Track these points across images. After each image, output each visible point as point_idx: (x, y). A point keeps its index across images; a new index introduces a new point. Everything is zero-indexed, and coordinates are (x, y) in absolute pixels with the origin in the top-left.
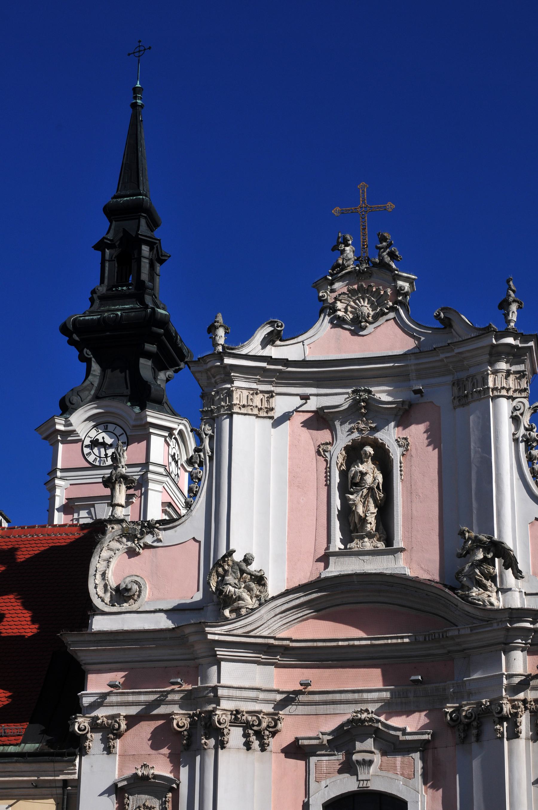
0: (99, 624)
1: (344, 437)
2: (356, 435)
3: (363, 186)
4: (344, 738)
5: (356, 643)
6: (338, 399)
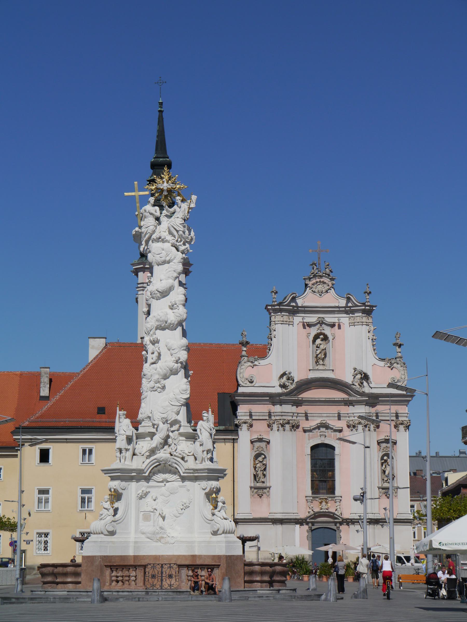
0: (241, 390)
1: (314, 331)
2: (319, 331)
4: (318, 427)
5: (321, 399)
6: (312, 318)
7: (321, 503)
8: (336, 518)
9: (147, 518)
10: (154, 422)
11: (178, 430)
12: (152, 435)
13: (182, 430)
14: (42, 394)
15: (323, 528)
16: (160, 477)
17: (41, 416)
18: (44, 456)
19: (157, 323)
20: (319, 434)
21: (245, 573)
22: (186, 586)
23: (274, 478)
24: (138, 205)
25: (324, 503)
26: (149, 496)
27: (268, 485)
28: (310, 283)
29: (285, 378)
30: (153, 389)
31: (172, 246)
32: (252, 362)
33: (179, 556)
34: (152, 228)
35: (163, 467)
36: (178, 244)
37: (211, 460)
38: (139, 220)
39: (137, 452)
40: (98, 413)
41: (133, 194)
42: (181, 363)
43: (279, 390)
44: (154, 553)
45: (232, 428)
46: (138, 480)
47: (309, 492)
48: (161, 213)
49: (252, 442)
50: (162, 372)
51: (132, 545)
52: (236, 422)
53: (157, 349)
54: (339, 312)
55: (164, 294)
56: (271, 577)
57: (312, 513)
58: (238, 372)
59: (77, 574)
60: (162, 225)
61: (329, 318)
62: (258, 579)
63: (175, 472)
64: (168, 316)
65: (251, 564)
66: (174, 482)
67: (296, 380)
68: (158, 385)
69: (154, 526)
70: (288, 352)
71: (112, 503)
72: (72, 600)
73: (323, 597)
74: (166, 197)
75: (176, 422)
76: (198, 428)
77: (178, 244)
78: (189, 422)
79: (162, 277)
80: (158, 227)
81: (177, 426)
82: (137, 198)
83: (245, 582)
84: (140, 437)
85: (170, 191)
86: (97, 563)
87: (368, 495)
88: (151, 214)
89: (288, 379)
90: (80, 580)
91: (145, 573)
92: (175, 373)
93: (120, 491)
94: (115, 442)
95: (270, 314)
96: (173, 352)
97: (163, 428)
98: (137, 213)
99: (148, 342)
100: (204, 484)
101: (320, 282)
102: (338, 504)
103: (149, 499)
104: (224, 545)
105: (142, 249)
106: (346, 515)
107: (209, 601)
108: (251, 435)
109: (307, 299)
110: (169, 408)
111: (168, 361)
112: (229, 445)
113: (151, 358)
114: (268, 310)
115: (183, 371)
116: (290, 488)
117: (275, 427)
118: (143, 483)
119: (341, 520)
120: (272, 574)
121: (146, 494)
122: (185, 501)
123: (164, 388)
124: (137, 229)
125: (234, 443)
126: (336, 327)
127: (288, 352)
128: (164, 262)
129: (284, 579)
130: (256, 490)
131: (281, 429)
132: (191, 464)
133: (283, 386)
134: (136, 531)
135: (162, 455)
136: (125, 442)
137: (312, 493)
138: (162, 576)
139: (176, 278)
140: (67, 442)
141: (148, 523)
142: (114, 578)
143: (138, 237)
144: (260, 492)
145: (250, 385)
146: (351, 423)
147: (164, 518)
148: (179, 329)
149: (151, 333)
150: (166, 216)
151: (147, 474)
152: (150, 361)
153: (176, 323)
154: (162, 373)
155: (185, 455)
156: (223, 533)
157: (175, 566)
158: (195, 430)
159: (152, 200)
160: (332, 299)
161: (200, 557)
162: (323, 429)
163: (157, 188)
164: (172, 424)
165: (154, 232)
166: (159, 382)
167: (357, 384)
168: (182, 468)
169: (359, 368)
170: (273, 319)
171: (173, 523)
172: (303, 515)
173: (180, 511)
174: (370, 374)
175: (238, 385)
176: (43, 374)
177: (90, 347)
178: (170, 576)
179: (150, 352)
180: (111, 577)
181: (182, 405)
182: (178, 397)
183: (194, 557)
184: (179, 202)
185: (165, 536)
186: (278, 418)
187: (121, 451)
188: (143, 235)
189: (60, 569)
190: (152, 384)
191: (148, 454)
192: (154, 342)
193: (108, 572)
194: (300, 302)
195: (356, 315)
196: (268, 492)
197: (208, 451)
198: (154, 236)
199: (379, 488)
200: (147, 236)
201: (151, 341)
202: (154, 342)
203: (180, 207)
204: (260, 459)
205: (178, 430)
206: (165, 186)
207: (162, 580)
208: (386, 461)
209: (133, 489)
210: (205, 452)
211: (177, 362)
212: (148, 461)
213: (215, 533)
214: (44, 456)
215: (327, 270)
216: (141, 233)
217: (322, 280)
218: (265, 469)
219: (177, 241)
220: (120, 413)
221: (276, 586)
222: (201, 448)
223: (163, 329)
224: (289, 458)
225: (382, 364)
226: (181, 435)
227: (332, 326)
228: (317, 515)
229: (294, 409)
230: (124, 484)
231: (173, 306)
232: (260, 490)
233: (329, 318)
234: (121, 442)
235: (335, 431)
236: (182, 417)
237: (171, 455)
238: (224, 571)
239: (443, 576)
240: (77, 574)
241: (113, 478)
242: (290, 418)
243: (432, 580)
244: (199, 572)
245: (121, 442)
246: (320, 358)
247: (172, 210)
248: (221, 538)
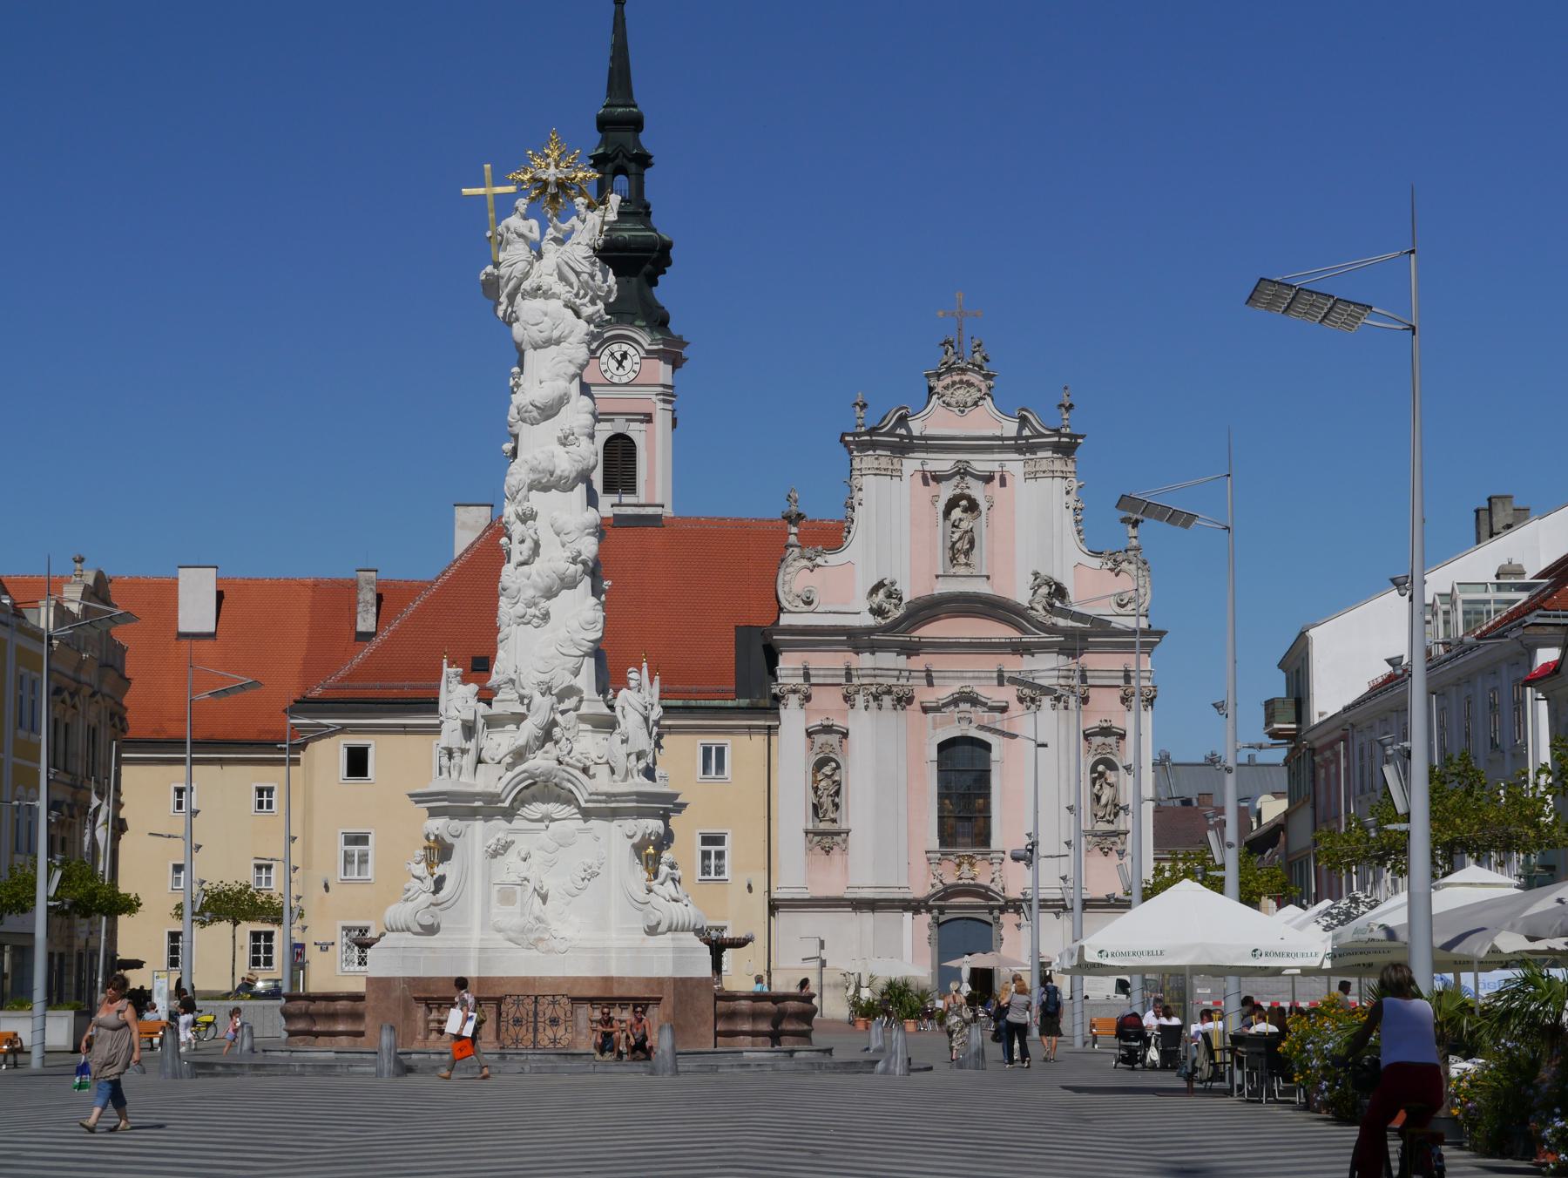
1: (947, 491)
2: (958, 491)
4: (955, 701)
7: (959, 865)
8: (993, 899)
9: (507, 897)
10: (523, 692)
11: (576, 709)
12: (518, 719)
13: (584, 709)
14: (361, 627)
15: (963, 918)
16: (537, 809)
17: (350, 677)
18: (357, 763)
19: (532, 476)
20: (956, 716)
21: (718, 1016)
22: (586, 1042)
23: (858, 812)
24: (491, 215)
25: (966, 867)
26: (512, 851)
27: (844, 827)
28: (939, 386)
29: (881, 593)
30: (523, 620)
31: (566, 306)
32: (810, 559)
33: (576, 979)
34: (521, 266)
35: (542, 789)
36: (578, 301)
37: (649, 773)
38: (494, 250)
39: (485, 755)
40: (474, 670)
41: (481, 191)
42: (584, 563)
43: (869, 620)
44: (523, 973)
45: (767, 702)
46: (488, 817)
47: (934, 843)
48: (543, 234)
49: (809, 734)
50: (543, 583)
51: (474, 954)
52: (775, 690)
53: (531, 532)
54: (1004, 449)
55: (548, 411)
56: (775, 1024)
57: (940, 886)
58: (780, 581)
59: (357, 1016)
60: (544, 261)
61: (981, 463)
62: (747, 1027)
63: (569, 799)
64: (556, 461)
65: (732, 997)
66: (567, 822)
67: (906, 599)
68: (533, 611)
69: (523, 915)
70: (890, 536)
71: (430, 865)
72: (339, 1070)
73: (880, 1066)
74: (554, 197)
75: (570, 691)
76: (618, 703)
77: (578, 301)
78: (602, 689)
79: (544, 374)
80: (536, 265)
81: (575, 700)
82: (490, 200)
83: (717, 1034)
84: (492, 722)
85: (562, 185)
86: (397, 993)
87: (1042, 850)
88: (521, 236)
89: (889, 596)
90: (362, 1028)
91: (499, 1014)
92: (571, 584)
93: (449, 840)
94: (439, 733)
95: (851, 452)
96: (566, 539)
97: (542, 703)
98: (489, 234)
99: (513, 518)
100: (630, 825)
101: (961, 382)
102: (996, 867)
103: (512, 857)
104: (670, 955)
105: (500, 314)
106: (1013, 893)
107: (631, 1075)
108: (807, 719)
109: (932, 421)
110: (557, 662)
111: (555, 560)
112: (759, 740)
113: (518, 552)
114: (847, 444)
115: (587, 580)
116: (893, 830)
117: (860, 700)
118: (499, 823)
119: (1002, 902)
120: (778, 1018)
121: (507, 846)
122: (589, 861)
123: (546, 617)
124: (489, 269)
125: (769, 735)
126: (997, 481)
127: (890, 536)
128: (548, 343)
129: (806, 1027)
130: (817, 838)
131: (873, 704)
132: (603, 782)
133: (878, 611)
134: (484, 925)
135: (540, 762)
136: (459, 733)
137: (941, 844)
138: (536, 1022)
139: (574, 376)
140: (406, 733)
141: (509, 908)
142: (433, 1025)
143: (491, 287)
144: (827, 841)
145: (806, 608)
147: (544, 898)
148: (581, 489)
149: (519, 497)
150: (555, 240)
151: (506, 804)
152: (516, 557)
153: (573, 474)
154: (541, 585)
155: (588, 763)
156: (669, 929)
157: (565, 1000)
158: (612, 708)
159: (522, 204)
160: (987, 421)
161: (621, 980)
162: (965, 706)
163: (534, 179)
164: (561, 697)
165: (526, 275)
166: (535, 604)
167: (1039, 607)
168: (584, 790)
170: (856, 464)
171: (565, 909)
172: (919, 891)
173: (581, 884)
174: (1069, 585)
175: (781, 610)
176: (362, 583)
177: (457, 524)
178: (554, 1022)
179: (515, 539)
180: (427, 1022)
181: (586, 655)
182: (577, 637)
183: (607, 980)
184: (582, 209)
185: (546, 936)
186: (866, 681)
187: (450, 753)
188: (502, 282)
189: (321, 1006)
190: (520, 608)
191: (508, 760)
192: (526, 518)
193: (420, 1011)
194: (916, 427)
195: (1040, 455)
196: (845, 841)
197: (640, 755)
198: (526, 285)
200: (511, 284)
201: (518, 516)
202: (526, 518)
203: (584, 221)
204: (827, 770)
205: (576, 709)
206: (551, 174)
207: (536, 1030)
208: (1102, 775)
209: (477, 835)
210: (633, 757)
211: (574, 561)
212: (510, 775)
213: (652, 931)
214: (357, 763)
216: (498, 277)
217: (965, 378)
218: (837, 793)
219: (577, 295)
220: (449, 671)
221: (788, 1043)
222: (625, 749)
223: (546, 488)
224: (890, 771)
226: (582, 719)
227: (988, 479)
228: (949, 892)
229: (901, 662)
230: (456, 824)
231: (566, 438)
232: (826, 835)
233: (981, 463)
234: (451, 735)
235: (992, 709)
236: (586, 680)
237: (560, 763)
238: (669, 1010)
239: (1150, 1020)
240: (357, 1016)
241: (433, 813)
242: (893, 681)
243: (1129, 1028)
244: (616, 1013)
245: (451, 735)
246: (961, 550)
247: (566, 226)
248: (665, 941)
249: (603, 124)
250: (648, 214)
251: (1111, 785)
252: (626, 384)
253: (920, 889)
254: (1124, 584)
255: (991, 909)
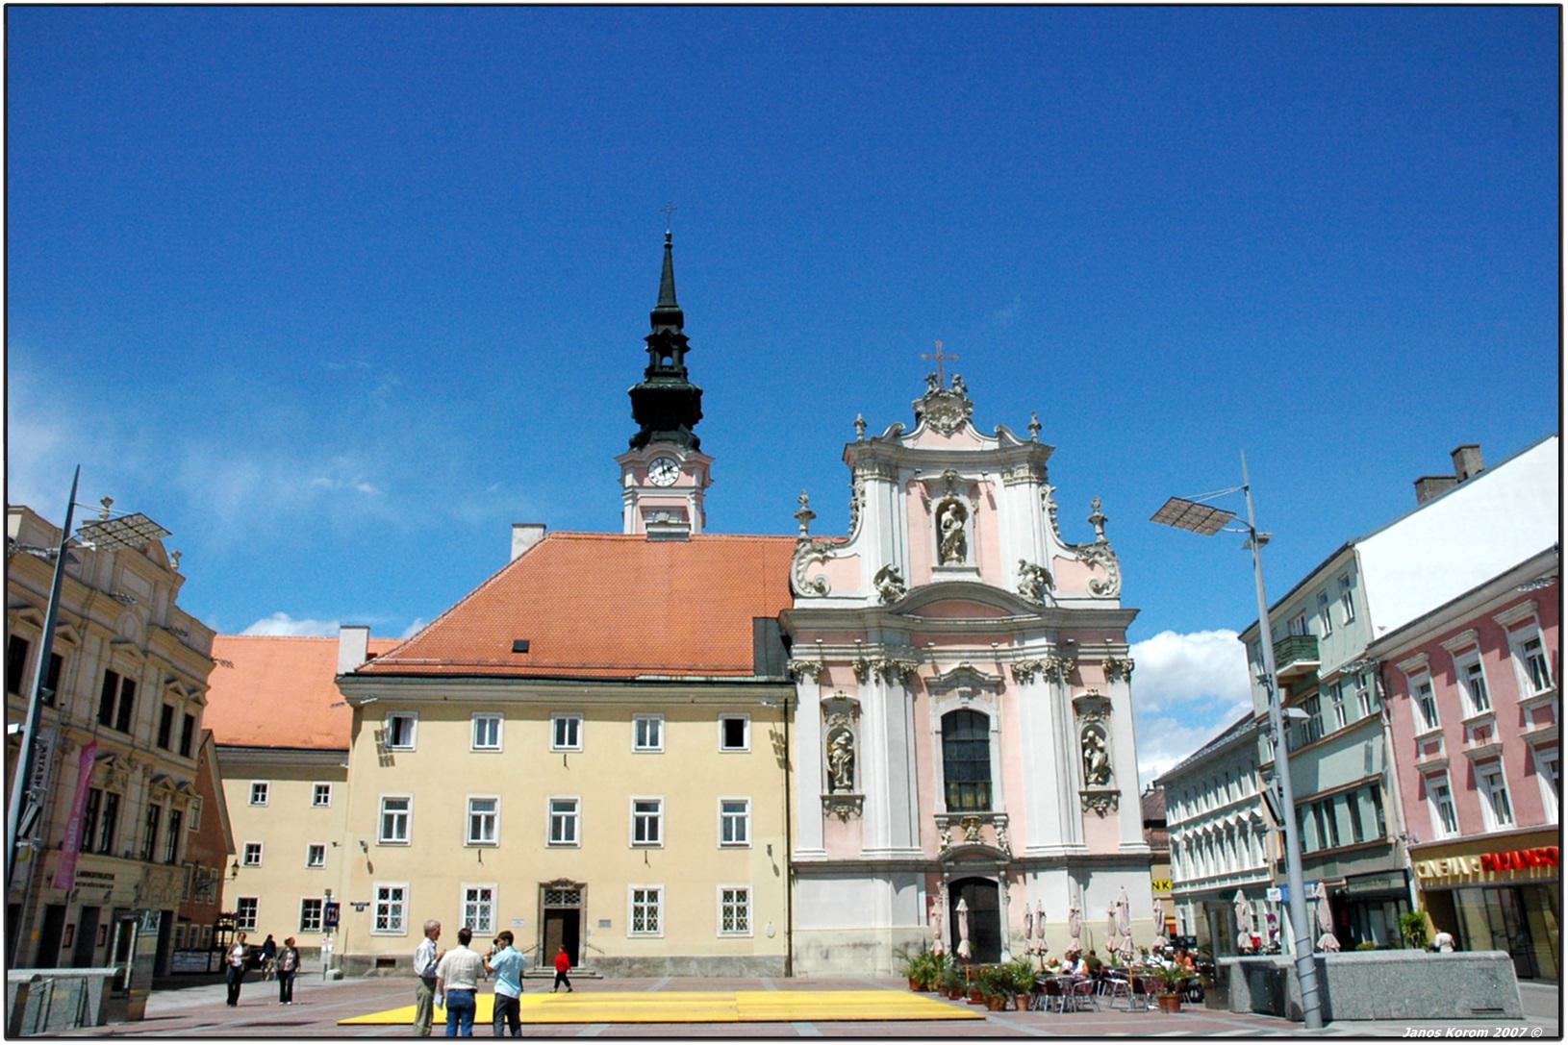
3: (939, 344)
23: (874, 778)
27: (857, 792)
29: (887, 580)
45: (783, 678)
47: (941, 807)
52: (792, 666)
106: (1019, 852)
109: (927, 440)
137: (950, 808)
144: (843, 809)
146: (1020, 667)
169: (1030, 561)
170: (859, 472)
175: (794, 595)
196: (861, 807)
199: (1081, 794)
204: (841, 740)
208: (1092, 740)
215: (958, 389)
218: (851, 761)
225: (1072, 555)
232: (841, 802)
246: (952, 546)
249: (657, 319)
250: (686, 375)
251: (1102, 750)
252: (670, 487)
253: (930, 850)
254: (1102, 574)
255: (999, 868)
